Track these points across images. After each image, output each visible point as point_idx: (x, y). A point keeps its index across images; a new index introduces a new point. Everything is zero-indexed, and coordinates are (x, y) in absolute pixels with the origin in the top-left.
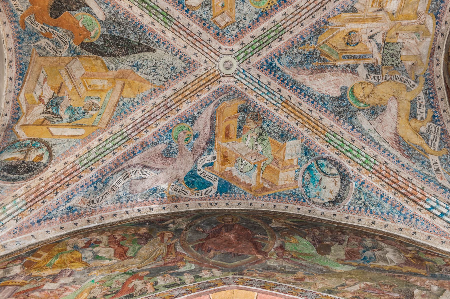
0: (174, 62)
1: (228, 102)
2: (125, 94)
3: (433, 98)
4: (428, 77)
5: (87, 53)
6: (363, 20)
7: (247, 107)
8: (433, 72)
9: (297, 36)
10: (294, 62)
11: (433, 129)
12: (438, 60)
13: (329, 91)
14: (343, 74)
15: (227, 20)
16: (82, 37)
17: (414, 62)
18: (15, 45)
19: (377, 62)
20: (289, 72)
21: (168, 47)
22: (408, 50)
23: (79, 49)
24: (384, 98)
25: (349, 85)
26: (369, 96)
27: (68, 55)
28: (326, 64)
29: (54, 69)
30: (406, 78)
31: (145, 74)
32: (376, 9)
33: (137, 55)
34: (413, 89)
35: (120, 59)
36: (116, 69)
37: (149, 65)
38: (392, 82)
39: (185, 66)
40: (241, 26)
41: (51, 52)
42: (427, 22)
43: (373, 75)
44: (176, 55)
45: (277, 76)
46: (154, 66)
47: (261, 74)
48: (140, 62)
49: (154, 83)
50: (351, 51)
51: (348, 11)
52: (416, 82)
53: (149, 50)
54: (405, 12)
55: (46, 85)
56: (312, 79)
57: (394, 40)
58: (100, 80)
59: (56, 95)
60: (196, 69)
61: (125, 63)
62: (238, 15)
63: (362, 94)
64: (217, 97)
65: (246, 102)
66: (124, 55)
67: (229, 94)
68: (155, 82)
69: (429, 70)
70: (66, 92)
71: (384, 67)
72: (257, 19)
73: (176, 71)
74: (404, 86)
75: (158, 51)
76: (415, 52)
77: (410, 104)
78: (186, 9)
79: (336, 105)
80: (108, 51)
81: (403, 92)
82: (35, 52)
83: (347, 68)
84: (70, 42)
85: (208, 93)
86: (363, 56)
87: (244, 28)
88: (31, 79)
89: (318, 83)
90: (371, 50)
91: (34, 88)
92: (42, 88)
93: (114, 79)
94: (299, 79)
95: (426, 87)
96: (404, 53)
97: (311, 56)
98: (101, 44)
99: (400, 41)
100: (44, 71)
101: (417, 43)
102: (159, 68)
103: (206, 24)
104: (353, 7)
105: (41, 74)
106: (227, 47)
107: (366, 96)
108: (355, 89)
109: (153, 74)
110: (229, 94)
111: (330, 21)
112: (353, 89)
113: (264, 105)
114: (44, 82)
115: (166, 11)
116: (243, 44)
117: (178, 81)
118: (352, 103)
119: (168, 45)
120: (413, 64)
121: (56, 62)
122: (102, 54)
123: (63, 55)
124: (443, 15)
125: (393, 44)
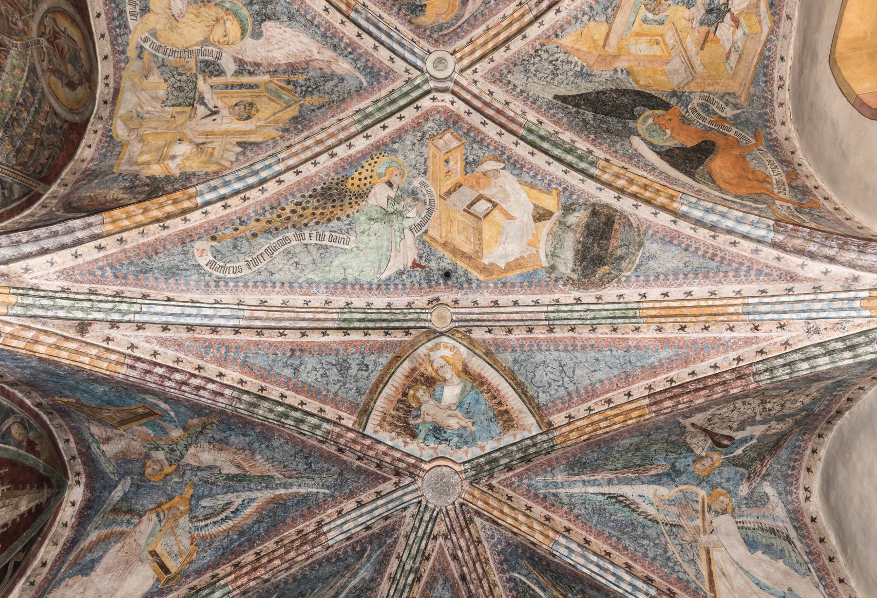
0: (525, 80)
1: (441, 21)
2: (604, 28)
4: (123, 57)
5: (660, 96)
6: (226, 133)
7: (412, 12)
8: (114, 67)
9: (333, 116)
10: (336, 80)
12: (107, 85)
13: (281, 31)
14: (259, 61)
15: (441, 141)
16: (667, 118)
17: (146, 81)
18: (773, 111)
19: (205, 80)
20: (343, 66)
21: (534, 103)
22: (155, 98)
23: (673, 101)
24: (192, 16)
25: (249, 41)
26: (217, 20)
27: (690, 93)
28: (286, 77)
29: (713, 73)
30: (157, 54)
31: (571, 63)
32: (209, 145)
33: (583, 91)
34: (147, 35)
35: (610, 86)
36: (616, 70)
37: (563, 77)
38: (180, 47)
39: (509, 76)
40: (419, 134)
41: (716, 99)
42: (126, 131)
43: (212, 59)
44: (522, 91)
45: (363, 60)
46: (557, 75)
47: (389, 64)
48: (579, 81)
49: (558, 47)
50: (246, 95)
51: (251, 144)
52: (142, 47)
53: (564, 99)
54: (161, 142)
55: (728, 46)
56: (307, 53)
57: (179, 109)
58: (643, 53)
59: (712, 29)
60: (491, 72)
61: (602, 79)
62: (424, 149)
63: (228, 24)
64: (459, 30)
65: (413, 21)
66: (604, 92)
67: (440, 33)
68: (555, 50)
70: (696, 34)
71: (194, 71)
72: (394, 142)
73: (522, 68)
74: (162, 40)
75: (550, 98)
76: (145, 96)
77: (152, 6)
78: (505, 157)
79: (269, 6)
80: (627, 96)
81: (162, 28)
82: (743, 99)
83: (252, 70)
84: (687, 111)
85: (473, 34)
86: (227, 87)
87: (414, 131)
88: (751, 57)
89: (299, 46)
90: (215, 96)
91: (746, 41)
92: (734, 42)
93: (620, 55)
94: (328, 54)
96: (162, 93)
97: (310, 89)
98: (638, 108)
99: (170, 109)
100: (730, 71)
101: (142, 107)
102: (548, 72)
103: (476, 138)
104: (245, 148)
105: (733, 65)
106: (442, 104)
107: (222, 22)
108: (239, 34)
109: (559, 62)
110: (440, 33)
111: (281, 133)
112: (242, 34)
113: (384, 15)
114: (730, 52)
115: (535, 151)
116: (417, 108)
117: (519, 51)
118: (244, 8)
119: (534, 106)
120: (146, 77)
121: (709, 85)
122: (638, 93)
123: (698, 94)
125: (180, 105)
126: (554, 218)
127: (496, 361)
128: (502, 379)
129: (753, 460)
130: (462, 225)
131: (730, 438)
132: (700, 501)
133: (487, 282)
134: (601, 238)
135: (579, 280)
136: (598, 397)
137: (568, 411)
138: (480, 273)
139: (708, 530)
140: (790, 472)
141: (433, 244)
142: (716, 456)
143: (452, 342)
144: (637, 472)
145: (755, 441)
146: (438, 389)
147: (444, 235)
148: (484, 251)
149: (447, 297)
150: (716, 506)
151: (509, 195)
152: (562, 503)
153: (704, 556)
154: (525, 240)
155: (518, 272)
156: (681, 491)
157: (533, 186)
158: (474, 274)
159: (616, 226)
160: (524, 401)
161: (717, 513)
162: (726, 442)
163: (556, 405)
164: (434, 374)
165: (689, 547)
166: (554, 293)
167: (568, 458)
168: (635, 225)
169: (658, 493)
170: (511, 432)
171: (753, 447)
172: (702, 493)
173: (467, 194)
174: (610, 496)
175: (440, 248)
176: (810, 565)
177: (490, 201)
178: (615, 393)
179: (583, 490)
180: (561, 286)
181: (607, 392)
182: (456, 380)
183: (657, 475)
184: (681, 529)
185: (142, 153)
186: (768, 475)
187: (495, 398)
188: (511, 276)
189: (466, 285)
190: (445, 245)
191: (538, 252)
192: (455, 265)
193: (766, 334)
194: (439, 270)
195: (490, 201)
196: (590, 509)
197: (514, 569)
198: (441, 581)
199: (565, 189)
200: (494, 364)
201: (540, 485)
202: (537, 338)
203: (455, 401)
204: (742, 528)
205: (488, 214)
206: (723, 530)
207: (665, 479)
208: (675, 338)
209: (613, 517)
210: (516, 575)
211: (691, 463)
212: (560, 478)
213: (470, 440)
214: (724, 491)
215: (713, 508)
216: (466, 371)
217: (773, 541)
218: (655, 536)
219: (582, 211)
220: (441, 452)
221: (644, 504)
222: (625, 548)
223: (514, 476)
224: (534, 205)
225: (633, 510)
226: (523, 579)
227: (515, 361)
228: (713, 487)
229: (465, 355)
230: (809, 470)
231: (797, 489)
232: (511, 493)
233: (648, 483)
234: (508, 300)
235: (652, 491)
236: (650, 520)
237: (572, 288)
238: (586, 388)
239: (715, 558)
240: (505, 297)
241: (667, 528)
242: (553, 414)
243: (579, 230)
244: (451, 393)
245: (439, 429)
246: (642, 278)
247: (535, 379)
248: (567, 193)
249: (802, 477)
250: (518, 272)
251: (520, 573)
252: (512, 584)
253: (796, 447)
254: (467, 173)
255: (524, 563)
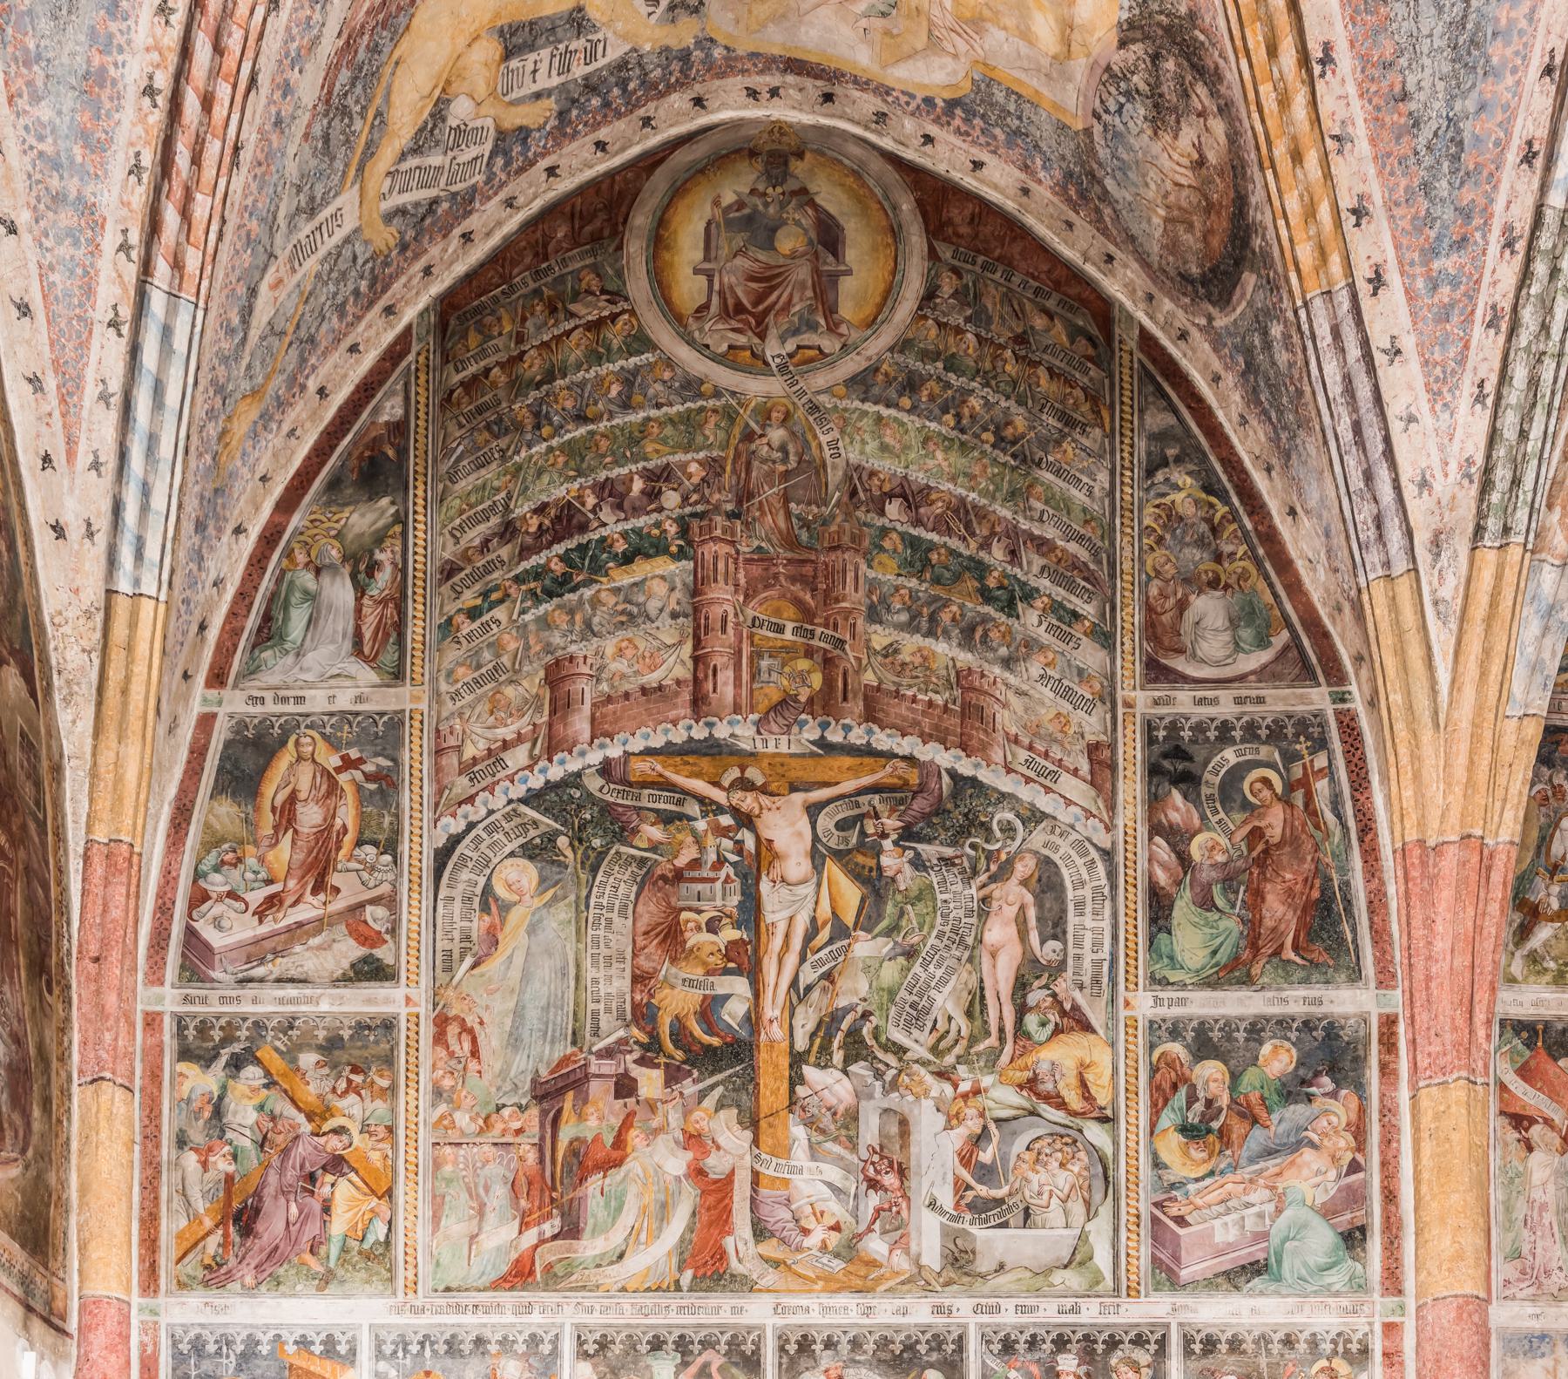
3: (606, 104)
11: (466, 155)
69: (726, 59)
95: (651, 62)
124: (958, 131)
185: (1026, 35)
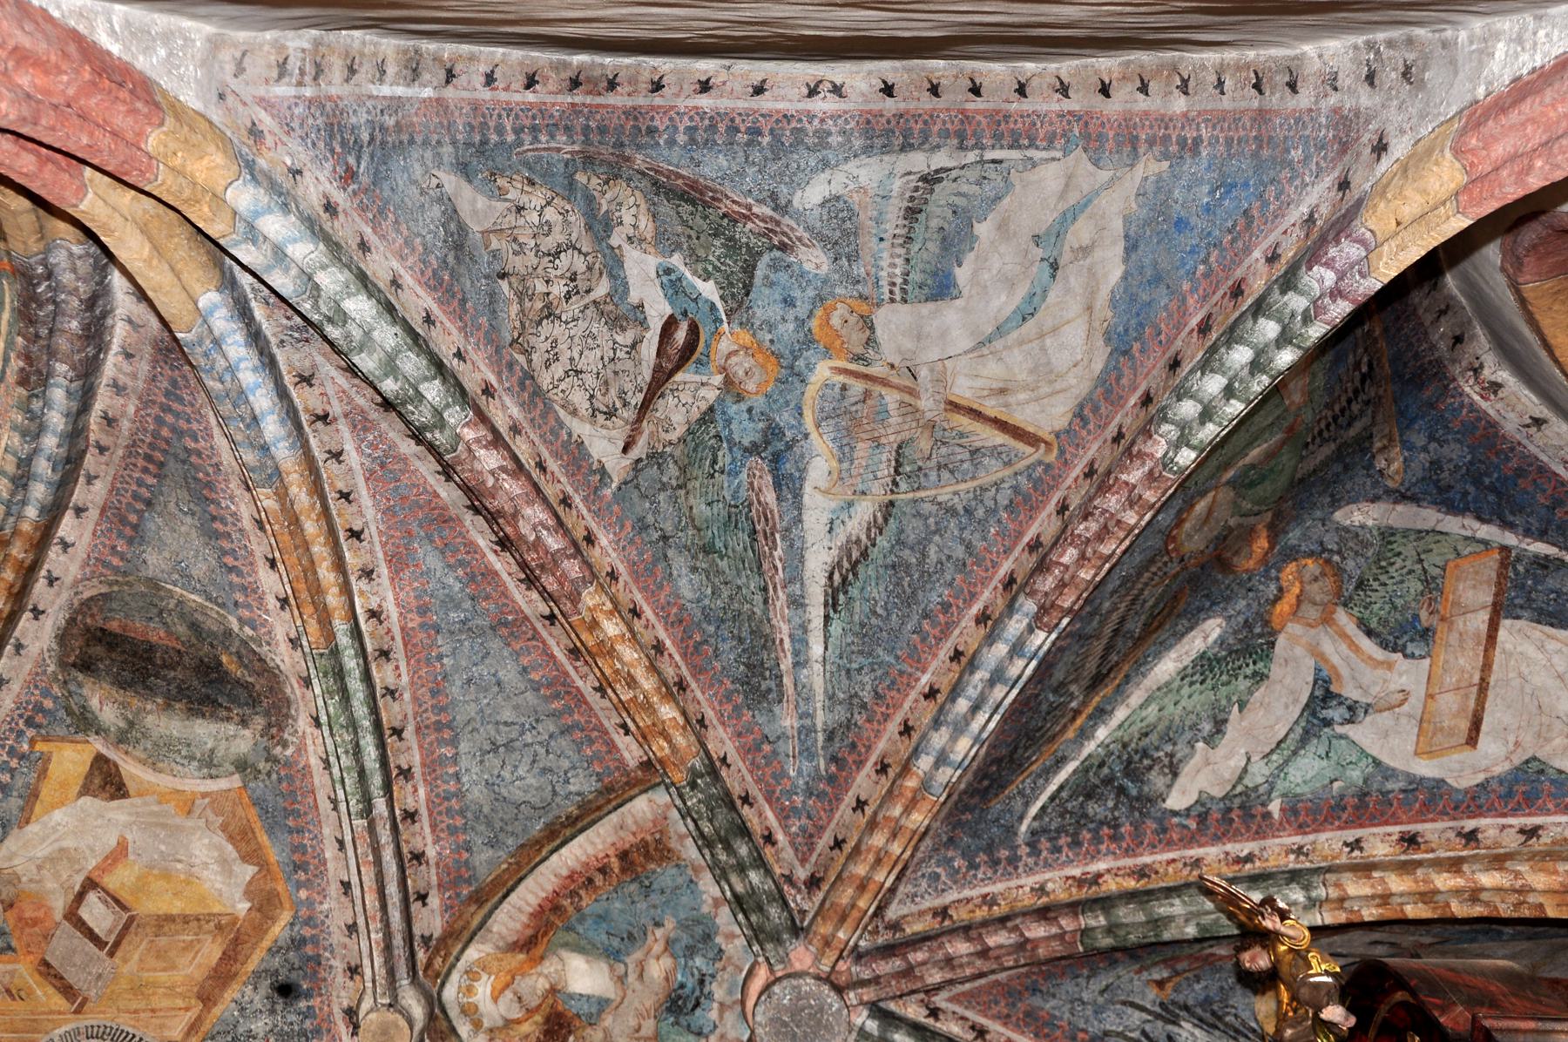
126: (112, 754)
127: (497, 883)
128: (542, 868)
129: (732, 245)
130: (151, 962)
131: (669, 326)
132: (841, 378)
133: (296, 905)
134: (150, 660)
135: (267, 714)
136: (566, 674)
137: (611, 730)
138: (274, 920)
139: (908, 382)
140: (766, 140)
141: (206, 1026)
142: (725, 345)
143: (455, 977)
144: (769, 537)
145: (676, 260)
146: (574, 1007)
147: (180, 1003)
148: (216, 910)
149: (341, 993)
150: (856, 339)
151: (62, 850)
152: (848, 725)
153: (964, 422)
154: (178, 821)
155: (263, 838)
156: (818, 426)
157: (32, 795)
158: (279, 930)
159: (114, 626)
160: (594, 822)
161: (871, 342)
162: (681, 335)
163: (597, 757)
164: (538, 1018)
165: (944, 450)
166: (307, 766)
167: (736, 708)
168: (104, 589)
169: (823, 485)
170: (673, 844)
171: (694, 258)
172: (822, 372)
173: (65, 946)
174: (832, 603)
175: (217, 1011)
176: (989, 155)
177: (80, 897)
178: (551, 642)
179: (818, 667)
180: (289, 752)
181: (553, 656)
182: (550, 967)
183: (777, 486)
184: (907, 451)
186: (774, 196)
187: (590, 881)
188: (275, 853)
189: (309, 950)
190: (207, 999)
191: (204, 795)
192: (257, 975)
193: (335, 402)
194: (273, 1012)
195: (80, 897)
196: (861, 659)
197: (1011, 831)
198: (1037, 1001)
199: (30, 722)
200: (505, 885)
201: (806, 766)
202: (428, 800)
203: (604, 966)
204: (904, 291)
205: (117, 901)
206: (908, 344)
207: (788, 467)
208: (383, 545)
209: (879, 611)
210: (1024, 828)
211: (744, 406)
212: (788, 721)
213: (699, 930)
214: (819, 312)
215: (859, 350)
216: (532, 943)
217: (934, 223)
218: (917, 523)
219: (85, 691)
220: (730, 992)
221: (849, 524)
222: (946, 607)
223: (785, 828)
224: (81, 794)
225: (865, 554)
226: (1034, 810)
227: (492, 844)
228: (809, 341)
229: (488, 948)
230: (759, 90)
231: (811, 117)
232: (826, 840)
233: (799, 506)
234: (336, 858)
235: (819, 497)
236: (886, 520)
237: (289, 730)
238: (547, 699)
239: (968, 394)
240: (330, 866)
241: (903, 486)
242: (621, 761)
243: (136, 703)
244: (583, 976)
245: (674, 1002)
246: (240, 597)
247: (536, 800)
248: (39, 719)
249: (781, 106)
250: (263, 838)
251: (1021, 818)
252: (1044, 844)
253: (693, 141)
254: (10, 948)
255: (996, 806)
